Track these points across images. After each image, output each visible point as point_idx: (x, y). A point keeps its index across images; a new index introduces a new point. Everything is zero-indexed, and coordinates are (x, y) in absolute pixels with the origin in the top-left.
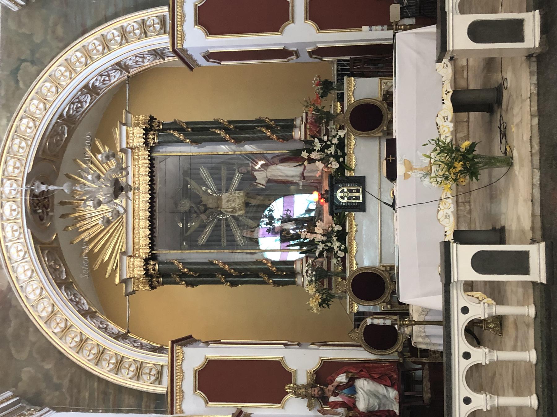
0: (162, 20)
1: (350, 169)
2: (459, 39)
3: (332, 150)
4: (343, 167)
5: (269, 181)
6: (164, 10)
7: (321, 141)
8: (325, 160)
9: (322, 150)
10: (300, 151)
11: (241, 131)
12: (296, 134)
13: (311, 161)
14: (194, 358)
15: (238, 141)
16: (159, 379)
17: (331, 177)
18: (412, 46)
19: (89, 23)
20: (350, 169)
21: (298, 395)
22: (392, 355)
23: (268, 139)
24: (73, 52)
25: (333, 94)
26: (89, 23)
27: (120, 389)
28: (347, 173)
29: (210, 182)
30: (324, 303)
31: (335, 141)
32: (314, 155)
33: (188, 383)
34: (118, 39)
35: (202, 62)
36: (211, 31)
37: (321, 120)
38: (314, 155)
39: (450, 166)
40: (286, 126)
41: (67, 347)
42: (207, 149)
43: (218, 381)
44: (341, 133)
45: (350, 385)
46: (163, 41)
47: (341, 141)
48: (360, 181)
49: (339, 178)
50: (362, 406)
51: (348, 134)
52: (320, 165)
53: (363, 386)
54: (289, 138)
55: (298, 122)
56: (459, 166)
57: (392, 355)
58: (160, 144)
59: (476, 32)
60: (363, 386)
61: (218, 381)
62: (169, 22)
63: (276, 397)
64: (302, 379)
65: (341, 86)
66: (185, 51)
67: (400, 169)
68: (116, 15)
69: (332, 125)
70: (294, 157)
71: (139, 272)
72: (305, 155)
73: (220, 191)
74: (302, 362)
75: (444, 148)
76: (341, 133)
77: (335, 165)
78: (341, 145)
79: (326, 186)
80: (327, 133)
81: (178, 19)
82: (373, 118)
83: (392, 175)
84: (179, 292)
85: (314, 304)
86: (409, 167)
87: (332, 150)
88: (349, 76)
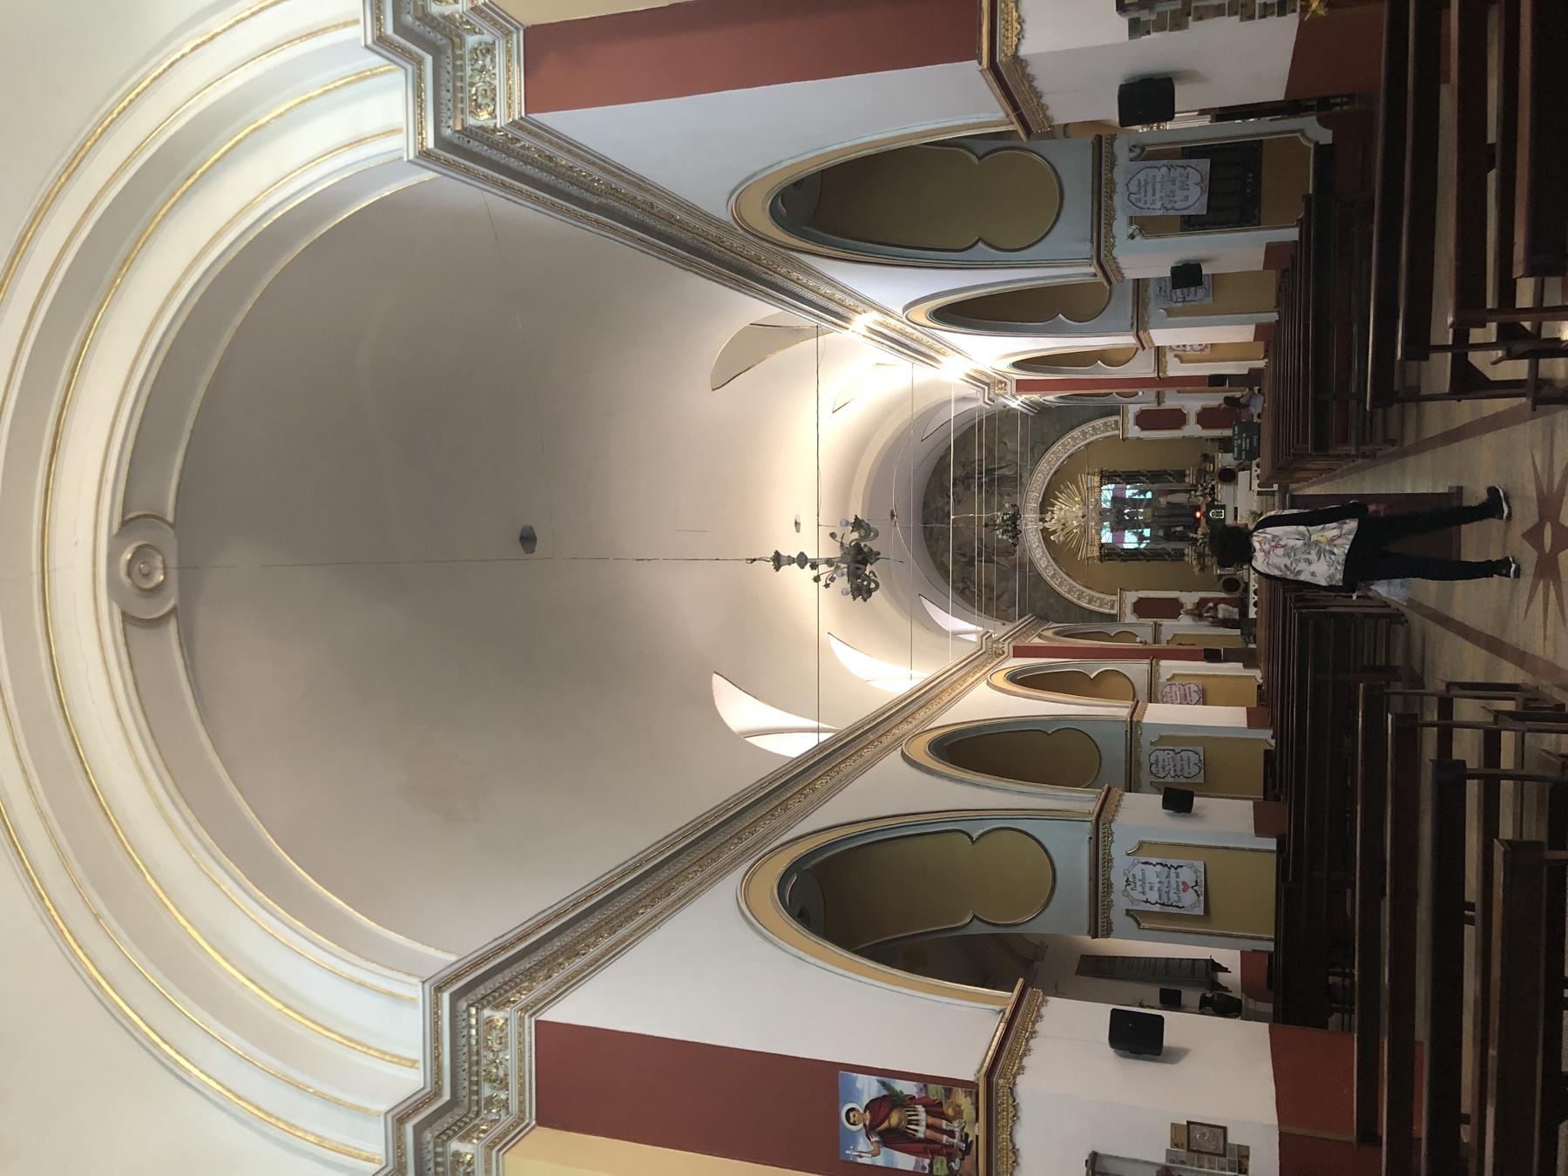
4: (1214, 500)
14: (1132, 597)
16: (1112, 607)
21: (1187, 613)
22: (1237, 594)
24: (1067, 439)
27: (1091, 612)
30: (1202, 570)
33: (1128, 609)
36: (1143, 429)
37: (1201, 473)
40: (1181, 475)
41: (1062, 591)
43: (1142, 608)
45: (1215, 608)
48: (1223, 507)
49: (1211, 506)
50: (1220, 616)
53: (1221, 606)
57: (1237, 594)
60: (1221, 606)
61: (1142, 608)
63: (1175, 616)
64: (1189, 606)
71: (1096, 554)
74: (1189, 599)
78: (1213, 488)
79: (1204, 509)
84: (1118, 564)
85: (1196, 570)
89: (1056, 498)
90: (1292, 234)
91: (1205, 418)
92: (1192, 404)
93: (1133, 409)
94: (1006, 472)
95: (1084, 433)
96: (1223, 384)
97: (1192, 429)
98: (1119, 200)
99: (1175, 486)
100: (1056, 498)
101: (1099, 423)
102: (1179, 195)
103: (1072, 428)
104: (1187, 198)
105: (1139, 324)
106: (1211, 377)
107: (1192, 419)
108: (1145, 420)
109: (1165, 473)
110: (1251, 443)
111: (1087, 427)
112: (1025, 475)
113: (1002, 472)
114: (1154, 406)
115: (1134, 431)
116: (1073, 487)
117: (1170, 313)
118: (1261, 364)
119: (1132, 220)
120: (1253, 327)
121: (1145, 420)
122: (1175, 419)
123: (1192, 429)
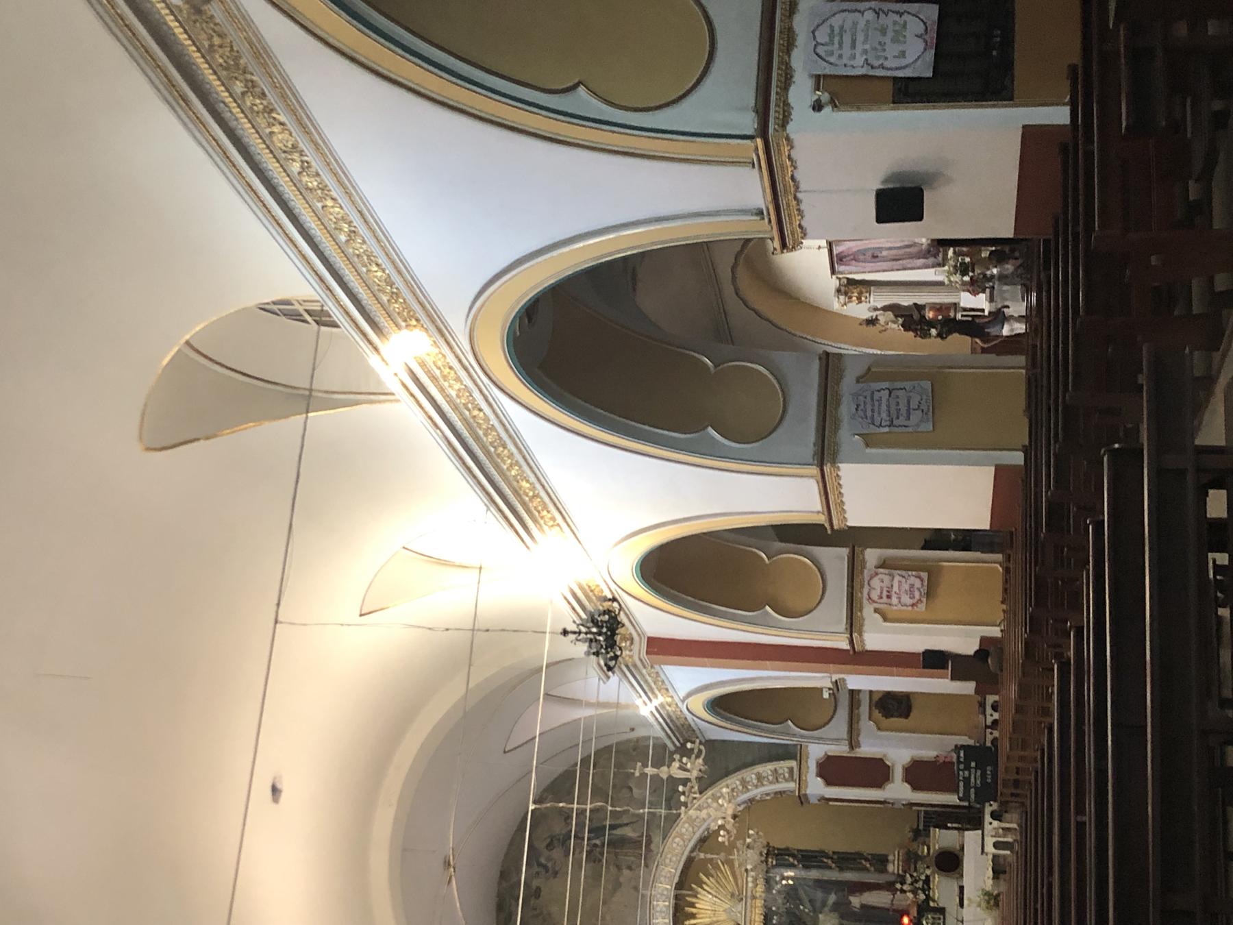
0: (791, 770)
1: (934, 901)
2: (990, 848)
3: (920, 884)
4: (928, 898)
5: (863, 906)
6: (793, 764)
7: (911, 876)
8: (914, 892)
9: (912, 884)
10: (893, 883)
11: (845, 860)
12: (890, 868)
13: (903, 891)
15: (841, 869)
17: (919, 906)
18: (971, 837)
19: (731, 768)
20: (934, 901)
23: (867, 870)
25: (921, 839)
26: (731, 768)
28: (932, 904)
29: (808, 905)
31: (923, 877)
32: (905, 887)
34: (755, 782)
35: (813, 800)
36: (829, 783)
37: (911, 859)
38: (905, 887)
39: (988, 902)
40: (881, 862)
42: (814, 874)
44: (928, 872)
46: (792, 786)
47: (928, 877)
48: (942, 911)
51: (933, 873)
52: (910, 895)
54: (884, 870)
55: (891, 858)
56: (992, 902)
58: (778, 865)
59: (996, 845)
62: (796, 776)
65: (928, 836)
66: (805, 795)
67: (966, 902)
68: (753, 764)
69: (919, 864)
70: (889, 887)
72: (898, 886)
73: (814, 911)
75: (987, 894)
76: (928, 872)
77: (922, 897)
79: (914, 912)
80: (916, 870)
81: (803, 770)
82: (950, 862)
83: (961, 905)
86: (969, 899)
87: (920, 884)
88: (935, 827)
89: (700, 884)
90: (1059, 115)
91: (918, 774)
92: (898, 748)
93: (816, 752)
94: (628, 832)
95: (744, 783)
96: (945, 667)
97: (898, 791)
98: (800, 60)
99: (871, 877)
100: (700, 884)
101: (766, 769)
102: (892, 50)
103: (727, 774)
104: (903, 54)
105: (825, 455)
106: (928, 653)
107: (898, 773)
108: (832, 770)
109: (859, 855)
110: (984, 775)
111: (750, 774)
112: (657, 839)
113: (618, 832)
114: (841, 749)
115: (816, 787)
116: (726, 869)
117: (869, 441)
118: (995, 632)
119: (819, 81)
120: (993, 469)
121: (832, 770)
122: (876, 772)
123: (898, 791)
